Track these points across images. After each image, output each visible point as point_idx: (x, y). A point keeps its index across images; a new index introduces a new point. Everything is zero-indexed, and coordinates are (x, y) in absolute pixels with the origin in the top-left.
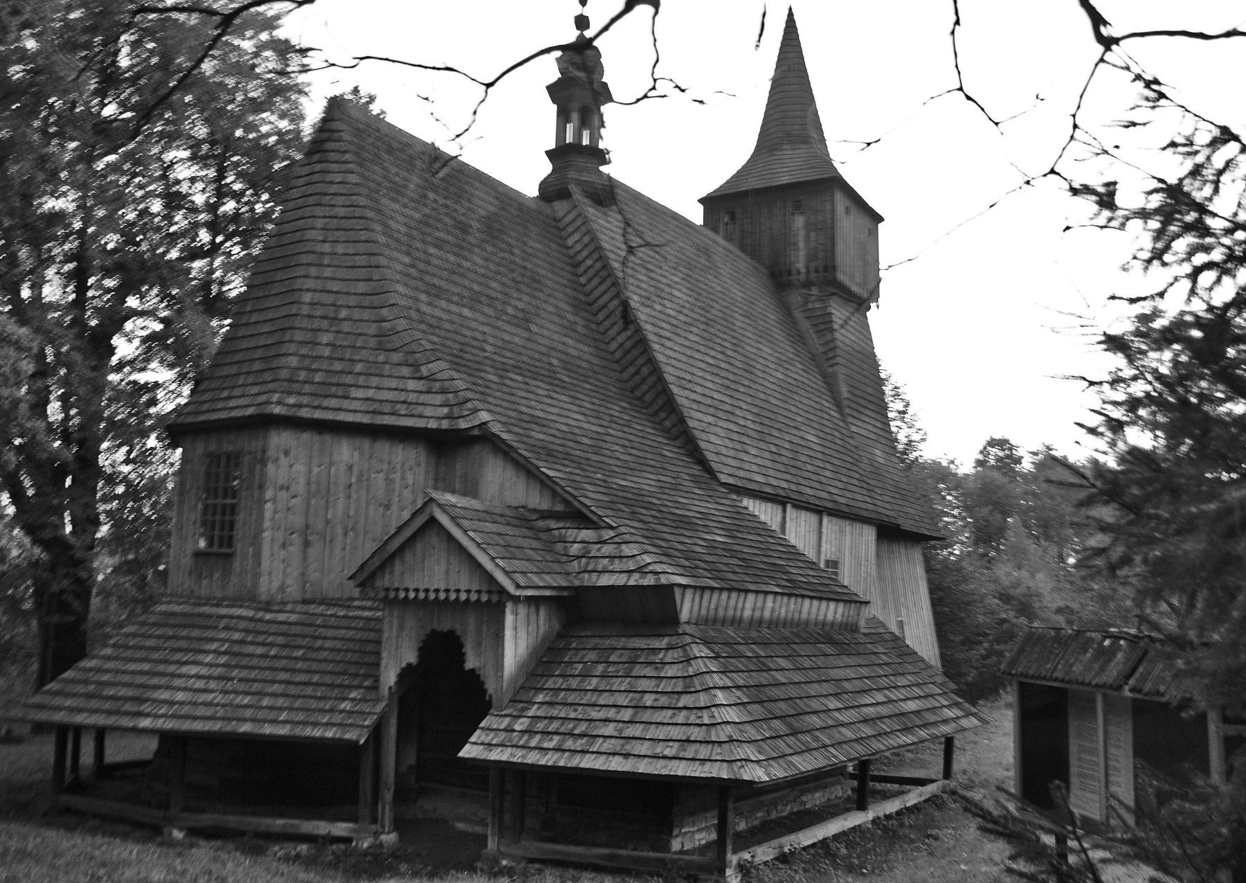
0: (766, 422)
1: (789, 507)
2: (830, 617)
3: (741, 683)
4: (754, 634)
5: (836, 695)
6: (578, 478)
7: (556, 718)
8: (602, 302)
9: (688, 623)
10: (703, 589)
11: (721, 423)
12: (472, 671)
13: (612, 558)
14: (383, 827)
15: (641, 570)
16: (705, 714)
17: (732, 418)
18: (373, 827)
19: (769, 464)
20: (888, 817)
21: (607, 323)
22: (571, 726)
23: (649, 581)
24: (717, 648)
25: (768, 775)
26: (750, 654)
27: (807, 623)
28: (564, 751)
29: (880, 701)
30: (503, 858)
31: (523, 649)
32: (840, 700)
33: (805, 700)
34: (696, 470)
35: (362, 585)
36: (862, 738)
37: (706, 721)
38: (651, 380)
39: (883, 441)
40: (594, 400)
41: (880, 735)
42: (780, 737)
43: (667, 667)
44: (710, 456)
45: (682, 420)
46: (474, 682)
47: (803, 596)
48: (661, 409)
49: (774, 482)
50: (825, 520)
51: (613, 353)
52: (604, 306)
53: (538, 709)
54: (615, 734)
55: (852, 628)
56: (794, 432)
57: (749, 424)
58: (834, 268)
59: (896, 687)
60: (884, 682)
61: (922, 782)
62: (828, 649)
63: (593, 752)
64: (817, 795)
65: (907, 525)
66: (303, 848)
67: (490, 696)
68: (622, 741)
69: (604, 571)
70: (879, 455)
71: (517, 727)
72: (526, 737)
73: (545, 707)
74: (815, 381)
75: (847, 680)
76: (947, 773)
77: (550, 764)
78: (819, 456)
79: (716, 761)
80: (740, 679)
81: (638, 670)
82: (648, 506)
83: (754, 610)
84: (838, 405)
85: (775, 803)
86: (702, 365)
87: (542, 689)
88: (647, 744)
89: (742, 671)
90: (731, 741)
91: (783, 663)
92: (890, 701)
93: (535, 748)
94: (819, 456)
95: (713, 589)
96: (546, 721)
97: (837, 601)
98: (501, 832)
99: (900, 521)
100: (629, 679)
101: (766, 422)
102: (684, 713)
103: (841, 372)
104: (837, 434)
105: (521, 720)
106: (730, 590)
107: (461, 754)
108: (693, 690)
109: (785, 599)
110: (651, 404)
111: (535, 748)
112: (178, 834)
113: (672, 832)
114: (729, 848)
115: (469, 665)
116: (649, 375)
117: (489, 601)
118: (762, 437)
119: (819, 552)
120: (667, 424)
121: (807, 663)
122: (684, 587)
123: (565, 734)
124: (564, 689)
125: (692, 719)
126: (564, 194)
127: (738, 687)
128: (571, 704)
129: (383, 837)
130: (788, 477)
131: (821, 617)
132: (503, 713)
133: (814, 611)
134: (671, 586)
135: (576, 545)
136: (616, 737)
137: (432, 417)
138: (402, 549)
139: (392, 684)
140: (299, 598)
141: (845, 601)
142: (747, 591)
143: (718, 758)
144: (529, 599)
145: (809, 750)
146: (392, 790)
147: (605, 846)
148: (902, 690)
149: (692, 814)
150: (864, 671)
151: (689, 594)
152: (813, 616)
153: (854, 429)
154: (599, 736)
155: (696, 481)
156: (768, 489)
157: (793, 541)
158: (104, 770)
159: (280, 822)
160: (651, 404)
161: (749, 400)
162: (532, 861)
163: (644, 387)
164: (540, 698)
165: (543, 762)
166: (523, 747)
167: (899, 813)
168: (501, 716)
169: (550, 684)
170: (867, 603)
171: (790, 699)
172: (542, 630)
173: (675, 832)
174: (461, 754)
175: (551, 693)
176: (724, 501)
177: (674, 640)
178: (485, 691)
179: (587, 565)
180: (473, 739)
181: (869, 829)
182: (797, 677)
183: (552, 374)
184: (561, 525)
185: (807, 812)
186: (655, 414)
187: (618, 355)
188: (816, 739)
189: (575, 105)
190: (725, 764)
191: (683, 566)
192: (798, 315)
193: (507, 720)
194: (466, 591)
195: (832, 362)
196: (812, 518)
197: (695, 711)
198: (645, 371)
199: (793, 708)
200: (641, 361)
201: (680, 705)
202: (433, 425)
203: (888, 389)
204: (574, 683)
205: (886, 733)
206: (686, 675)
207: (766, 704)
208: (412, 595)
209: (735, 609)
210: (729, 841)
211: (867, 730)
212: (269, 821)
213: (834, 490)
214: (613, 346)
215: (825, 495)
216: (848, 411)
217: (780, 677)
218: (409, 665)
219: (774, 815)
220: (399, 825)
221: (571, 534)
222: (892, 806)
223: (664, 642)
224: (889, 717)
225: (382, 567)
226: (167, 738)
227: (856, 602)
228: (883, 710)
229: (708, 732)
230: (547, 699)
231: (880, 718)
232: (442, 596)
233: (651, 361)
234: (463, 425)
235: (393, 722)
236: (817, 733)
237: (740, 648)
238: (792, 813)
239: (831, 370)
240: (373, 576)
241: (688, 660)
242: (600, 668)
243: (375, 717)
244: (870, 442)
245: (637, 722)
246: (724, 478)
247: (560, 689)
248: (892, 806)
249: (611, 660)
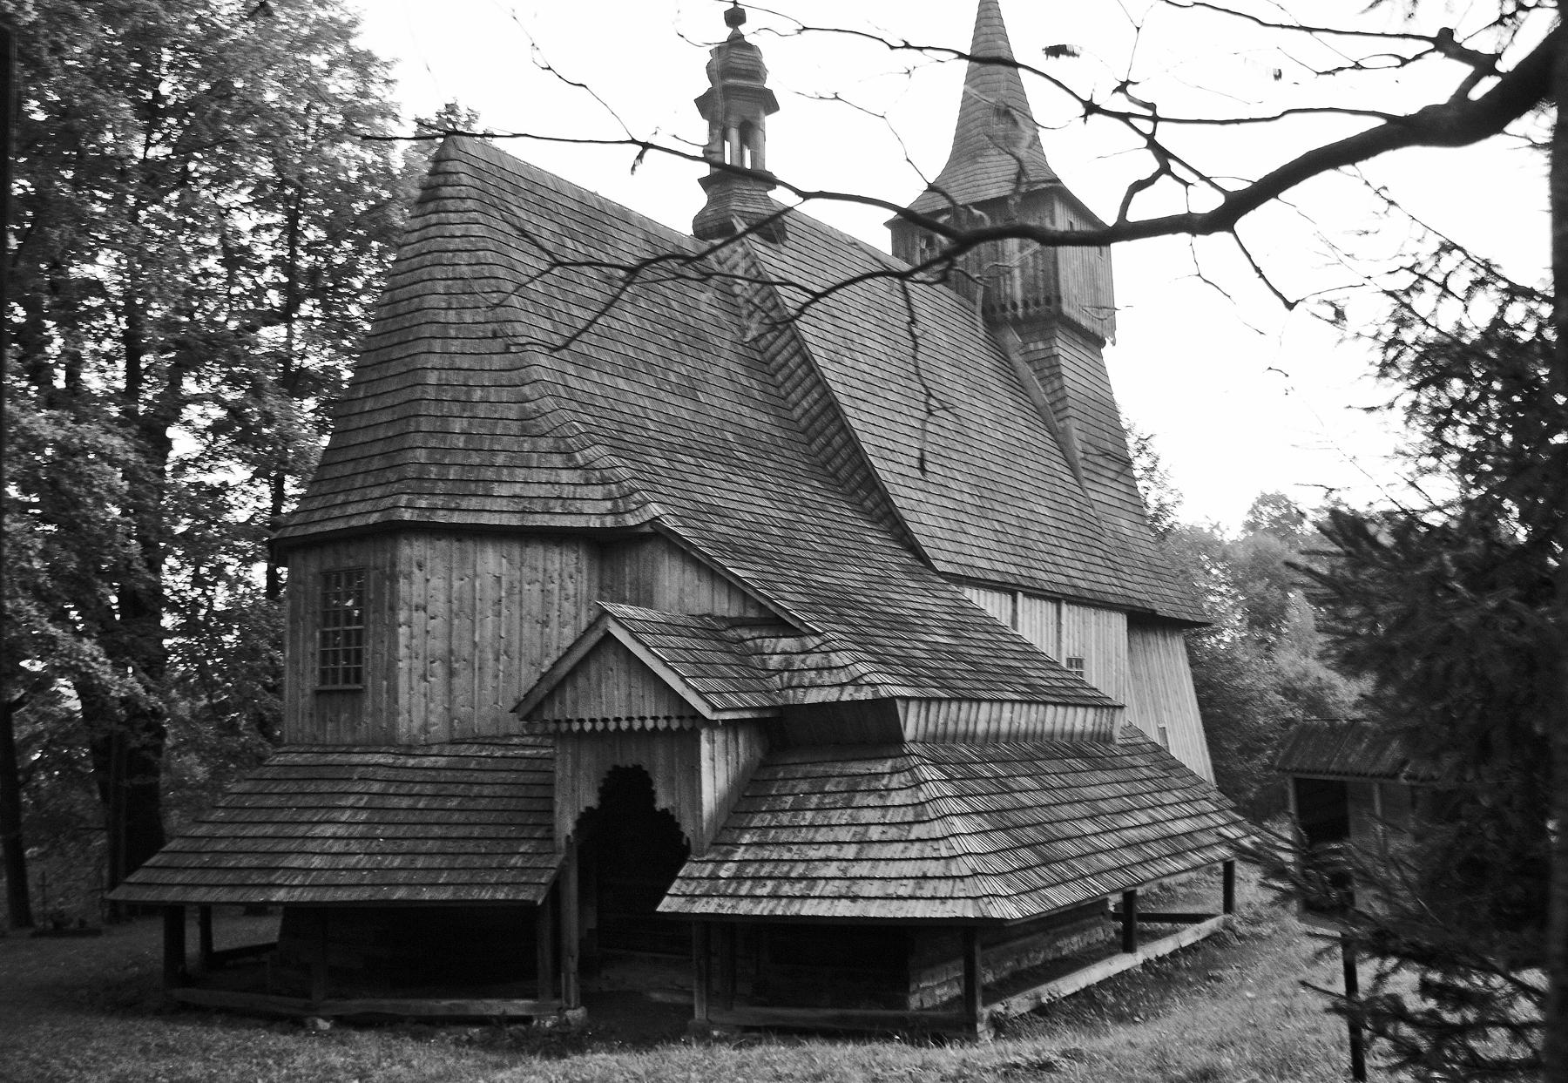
0: (986, 493)
1: (1020, 595)
2: (1078, 727)
3: (981, 807)
4: (991, 751)
5: (1092, 817)
6: (771, 577)
7: (768, 860)
8: (780, 359)
9: (914, 741)
10: (929, 700)
11: (932, 500)
12: (665, 811)
13: (819, 669)
14: (568, 1001)
15: (855, 682)
16: (942, 845)
17: (945, 492)
18: (557, 1002)
19: (994, 545)
20: (1160, 959)
21: (788, 385)
22: (786, 869)
23: (865, 694)
24: (949, 769)
25: (1021, 911)
26: (988, 774)
27: (1052, 735)
28: (780, 897)
29: (1144, 822)
31: (722, 783)
32: (1096, 823)
33: (1057, 825)
34: (907, 558)
35: (528, 718)
36: (1125, 866)
37: (944, 853)
38: (844, 453)
39: (1130, 508)
40: (781, 481)
41: (1146, 861)
42: (1031, 867)
43: (893, 793)
44: (922, 540)
45: (886, 498)
46: (668, 821)
47: (1045, 703)
48: (860, 486)
49: (1000, 567)
50: (1064, 608)
51: (797, 422)
52: (785, 364)
53: (746, 850)
54: (839, 874)
55: (1106, 738)
56: (1021, 504)
57: (967, 498)
58: (1059, 299)
59: (1162, 806)
60: (1147, 800)
61: (1197, 919)
62: (1077, 764)
63: (814, 897)
64: (1075, 939)
65: (1163, 610)
68: (847, 883)
69: (813, 686)
70: (1125, 525)
71: (723, 874)
72: (734, 885)
73: (753, 849)
74: (1043, 440)
75: (1103, 799)
76: (1229, 906)
77: (765, 913)
78: (1054, 532)
79: (959, 898)
80: (978, 803)
81: (859, 800)
82: (855, 606)
83: (989, 723)
84: (1072, 467)
85: (1025, 950)
86: (907, 430)
87: (748, 828)
88: (877, 883)
89: (981, 795)
90: (975, 874)
91: (1028, 783)
92: (1156, 822)
93: (746, 896)
94: (1054, 532)
95: (940, 700)
96: (756, 865)
97: (1086, 706)
98: (711, 998)
99: (1156, 606)
100: (849, 811)
101: (986, 493)
102: (917, 845)
103: (1073, 426)
104: (1073, 503)
105: (726, 866)
106: (960, 700)
107: (659, 909)
108: (926, 818)
109: (1025, 707)
110: (847, 481)
111: (746, 896)
112: (324, 1025)
113: (908, 987)
114: (979, 999)
116: (844, 445)
117: (680, 729)
118: (982, 513)
119: (1059, 649)
120: (868, 504)
121: (1055, 782)
122: (907, 699)
123: (780, 878)
124: (774, 827)
125: (928, 852)
126: (727, 233)
127: (978, 813)
128: (784, 844)
129: (569, 1013)
130: (1018, 560)
131: (1068, 728)
132: (705, 858)
133: (1059, 719)
134: (892, 700)
135: (775, 657)
136: (840, 878)
137: (593, 513)
138: (573, 673)
139: (570, 833)
140: (444, 737)
141: (1095, 707)
142: (979, 701)
143: (962, 894)
144: (727, 724)
145: (1065, 882)
146: (576, 958)
147: (833, 1006)
148: (1169, 809)
149: (932, 965)
150: (1124, 789)
151: (913, 707)
152: (1058, 727)
153: (1093, 495)
154: (820, 878)
155: (908, 571)
156: (994, 577)
157: (1028, 638)
158: (215, 961)
159: (445, 1003)
160: (847, 481)
161: (965, 469)
162: (748, 1029)
163: (838, 461)
164: (747, 838)
165: (757, 912)
166: (731, 896)
167: (1173, 954)
168: (702, 862)
169: (756, 822)
170: (1121, 707)
171: (1039, 824)
172: (742, 760)
173: (913, 987)
174: (659, 909)
175: (759, 832)
176: (944, 594)
177: (899, 762)
178: (682, 834)
179: (790, 679)
180: (672, 891)
181: (1138, 973)
182: (1044, 798)
183: (728, 452)
184: (755, 634)
185: (1064, 959)
186: (854, 492)
187: (804, 422)
188: (1072, 869)
189: (734, 120)
190: (970, 901)
191: (904, 676)
192: (1017, 359)
193: (710, 866)
194: (653, 718)
195: (1061, 415)
196: (1049, 608)
197: (930, 843)
198: (838, 441)
199: (1044, 835)
200: (833, 429)
201: (912, 837)
202: (595, 523)
203: (1131, 441)
204: (785, 819)
205: (1153, 859)
206: (916, 801)
207: (1012, 832)
208: (588, 726)
209: (967, 723)
210: (978, 991)
211: (1131, 857)
212: (432, 1003)
213: (1072, 572)
214: (797, 412)
215: (1063, 579)
216: (1084, 474)
217: (1025, 799)
218: (589, 809)
219: (1025, 964)
220: (586, 999)
221: (769, 644)
222: (1164, 947)
223: (887, 766)
224: (1156, 840)
225: (550, 695)
226: (292, 911)
227: (1108, 707)
228: (1149, 833)
229: (947, 867)
230: (755, 839)
231: (1146, 842)
232: (624, 725)
233: (845, 429)
234: (631, 521)
235: (573, 876)
236: (1073, 862)
237: (976, 767)
238: (1046, 962)
239: (1062, 424)
240: (539, 706)
241: (918, 784)
242: (815, 800)
243: (553, 872)
244: (1113, 511)
245: (862, 860)
246: (940, 567)
247: (769, 827)
248: (1164, 947)
249: (826, 789)
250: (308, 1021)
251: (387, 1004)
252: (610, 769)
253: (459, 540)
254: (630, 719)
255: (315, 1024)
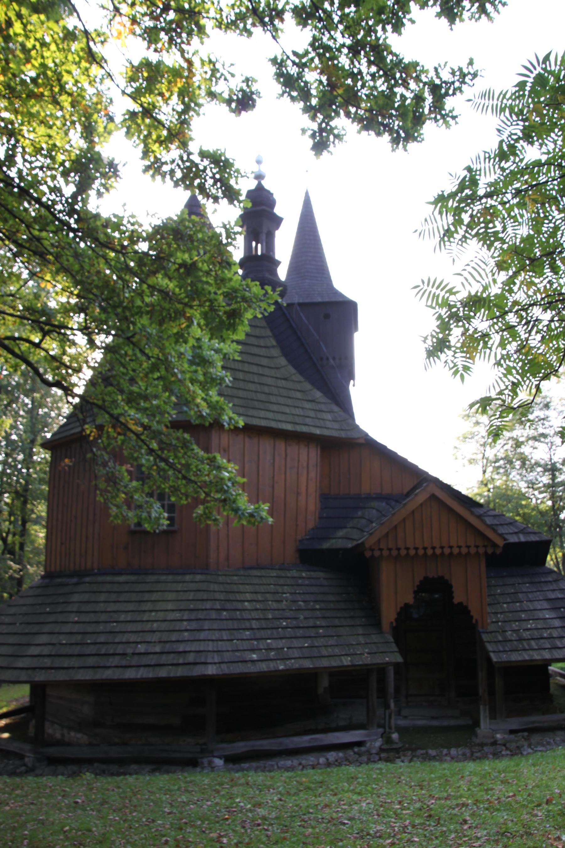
12: (461, 604)
30: (496, 733)
66: (332, 756)
67: (476, 620)
112: (219, 762)
115: (456, 601)
178: (472, 617)
250: (205, 761)
251: (266, 744)
252: (422, 579)
253: (250, 437)
254: (442, 548)
255: (210, 763)
